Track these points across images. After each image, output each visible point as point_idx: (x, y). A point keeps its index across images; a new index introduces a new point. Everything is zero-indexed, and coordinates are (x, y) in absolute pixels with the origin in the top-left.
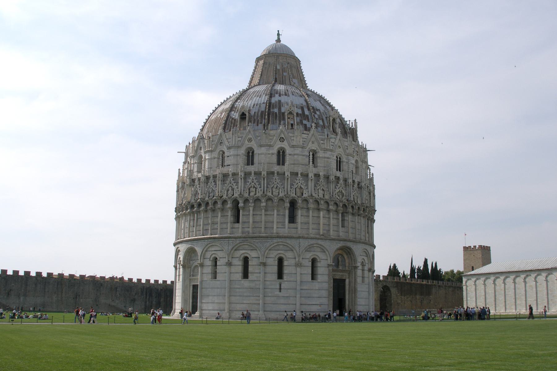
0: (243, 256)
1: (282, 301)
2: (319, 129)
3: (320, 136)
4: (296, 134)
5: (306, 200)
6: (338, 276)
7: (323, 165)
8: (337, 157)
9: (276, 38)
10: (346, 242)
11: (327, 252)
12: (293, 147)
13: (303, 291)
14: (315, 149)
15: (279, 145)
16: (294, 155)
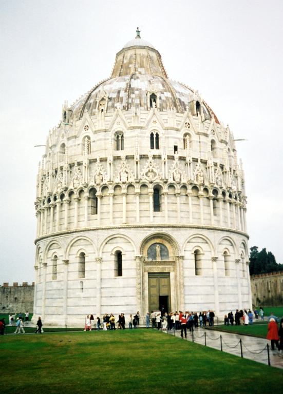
0: (54, 256)
1: (83, 303)
2: (133, 109)
3: (126, 115)
4: (99, 118)
5: (104, 188)
6: (156, 269)
7: (130, 146)
8: (152, 135)
9: (136, 34)
10: (158, 229)
11: (132, 243)
12: (96, 132)
13: (103, 290)
14: (121, 130)
15: (84, 133)
16: (98, 140)
